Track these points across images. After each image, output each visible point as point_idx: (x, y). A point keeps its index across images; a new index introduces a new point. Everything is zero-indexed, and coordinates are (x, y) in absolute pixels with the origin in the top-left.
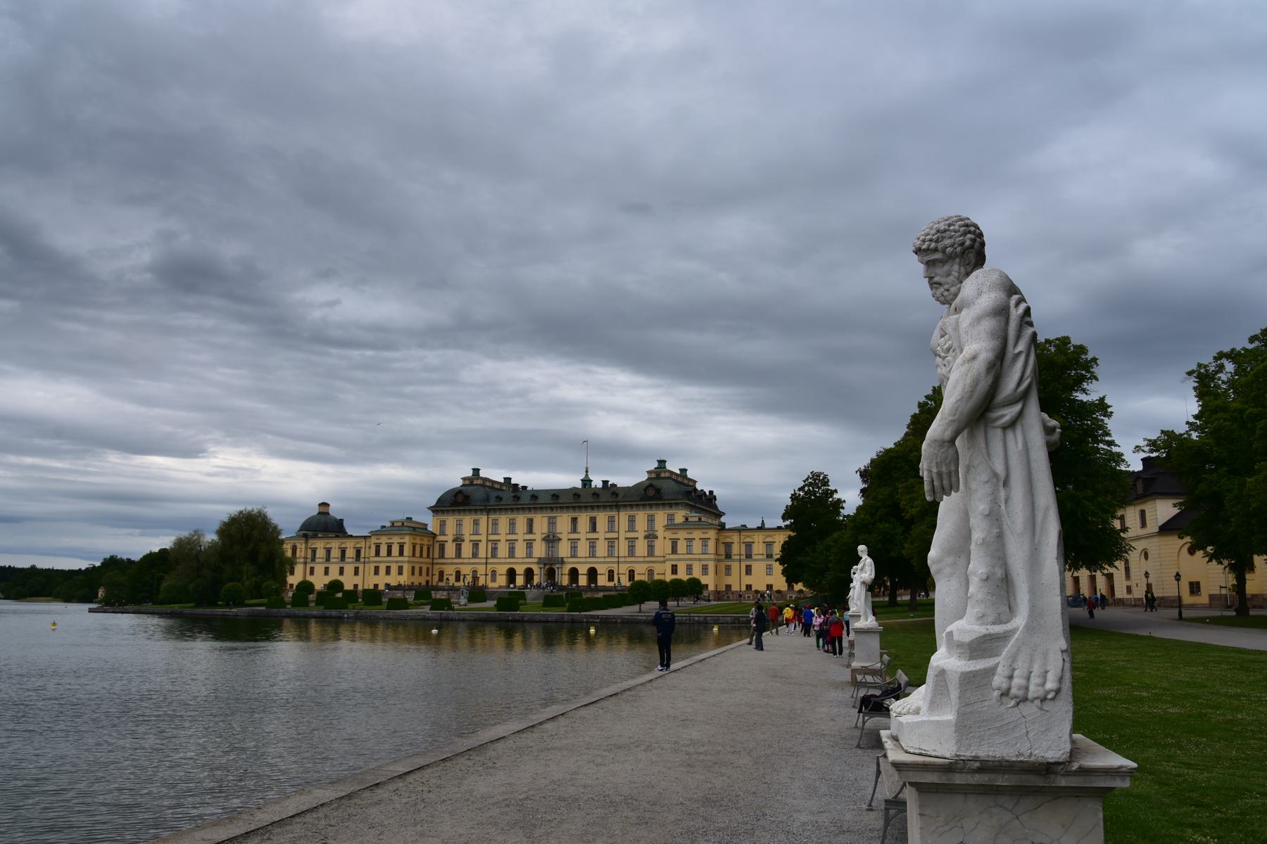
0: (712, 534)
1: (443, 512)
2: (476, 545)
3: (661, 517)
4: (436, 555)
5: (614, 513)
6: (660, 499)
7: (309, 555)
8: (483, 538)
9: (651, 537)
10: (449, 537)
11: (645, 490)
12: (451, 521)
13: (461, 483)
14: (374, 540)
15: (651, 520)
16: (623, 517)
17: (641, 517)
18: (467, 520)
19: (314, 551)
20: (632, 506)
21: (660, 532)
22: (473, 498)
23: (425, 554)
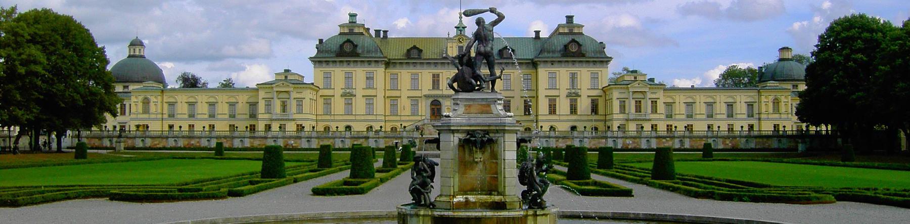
2: (370, 100)
3: (584, 74)
4: (320, 112)
6: (583, 56)
7: (166, 111)
8: (381, 95)
9: (573, 97)
10: (338, 92)
11: (566, 47)
12: (338, 73)
14: (262, 94)
15: (573, 77)
18: (359, 73)
19: (172, 105)
20: (552, 63)
22: (347, 48)
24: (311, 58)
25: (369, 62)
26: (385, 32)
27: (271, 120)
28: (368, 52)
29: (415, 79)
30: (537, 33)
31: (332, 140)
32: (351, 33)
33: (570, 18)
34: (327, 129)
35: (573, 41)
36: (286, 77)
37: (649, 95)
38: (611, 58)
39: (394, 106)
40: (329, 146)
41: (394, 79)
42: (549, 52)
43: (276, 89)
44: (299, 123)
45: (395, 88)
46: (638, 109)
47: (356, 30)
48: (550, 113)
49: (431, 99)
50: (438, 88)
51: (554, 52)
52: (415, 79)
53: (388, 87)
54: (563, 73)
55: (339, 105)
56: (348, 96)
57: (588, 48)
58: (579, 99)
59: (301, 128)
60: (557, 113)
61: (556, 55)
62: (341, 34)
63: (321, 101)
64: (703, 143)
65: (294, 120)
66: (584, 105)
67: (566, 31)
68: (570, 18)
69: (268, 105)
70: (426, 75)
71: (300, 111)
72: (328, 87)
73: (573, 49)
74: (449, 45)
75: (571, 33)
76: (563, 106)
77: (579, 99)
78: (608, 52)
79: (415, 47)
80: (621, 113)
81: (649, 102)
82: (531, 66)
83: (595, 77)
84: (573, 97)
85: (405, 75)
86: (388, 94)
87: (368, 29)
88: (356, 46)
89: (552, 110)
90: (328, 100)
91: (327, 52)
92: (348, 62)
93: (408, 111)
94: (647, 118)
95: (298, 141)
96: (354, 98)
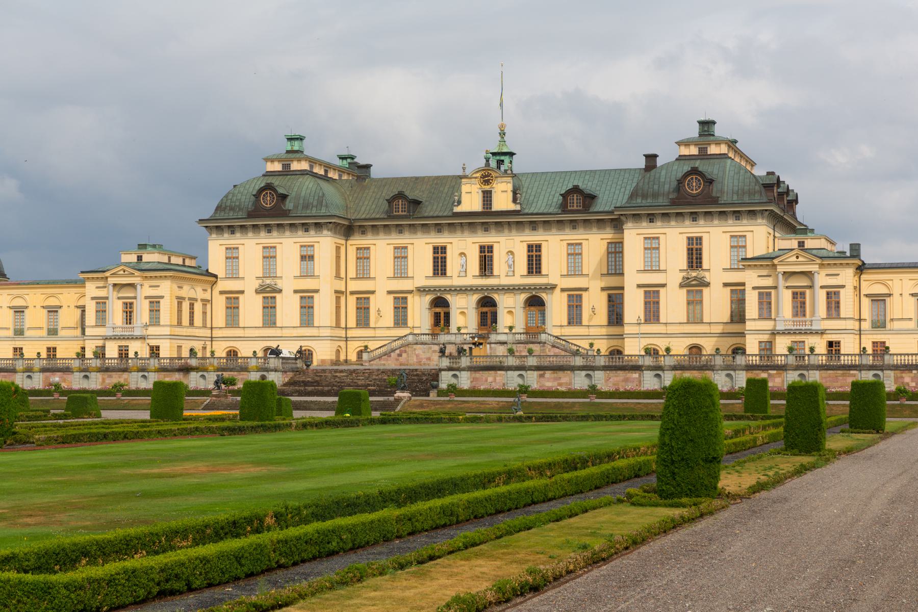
0: (847, 276)
1: (232, 230)
3: (717, 238)
6: (715, 201)
9: (695, 286)
16: (634, 237)
18: (288, 246)
20: (651, 218)
23: (198, 321)
25: (306, 227)
27: (106, 338)
28: (306, 206)
29: (401, 255)
30: (651, 158)
31: (125, 375)
34: (232, 354)
35: (694, 171)
36: (140, 258)
37: (822, 279)
39: (363, 311)
40: (175, 386)
41: (363, 256)
42: (645, 196)
43: (112, 281)
44: (154, 343)
45: (363, 274)
46: (800, 307)
47: (295, 166)
48: (647, 321)
49: (429, 298)
50: (444, 273)
51: (655, 195)
52: (401, 255)
53: (352, 273)
54: (674, 238)
55: (251, 308)
56: (269, 293)
57: (728, 183)
58: (706, 291)
59: (155, 351)
60: (663, 319)
61: (661, 201)
63: (220, 303)
64: (850, 380)
65: (143, 338)
66: (716, 303)
67: (694, 150)
69: (101, 312)
70: (421, 247)
71: (155, 320)
72: (233, 275)
73: (694, 188)
74: (465, 188)
76: (674, 304)
77: (706, 291)
79: (400, 195)
80: (761, 318)
81: (821, 295)
84: (695, 286)
85: (382, 248)
86: (354, 286)
88: (284, 197)
89: (652, 312)
91: (232, 209)
92: (269, 228)
93: (388, 318)
94: (815, 327)
95: (68, 377)
96: (278, 296)
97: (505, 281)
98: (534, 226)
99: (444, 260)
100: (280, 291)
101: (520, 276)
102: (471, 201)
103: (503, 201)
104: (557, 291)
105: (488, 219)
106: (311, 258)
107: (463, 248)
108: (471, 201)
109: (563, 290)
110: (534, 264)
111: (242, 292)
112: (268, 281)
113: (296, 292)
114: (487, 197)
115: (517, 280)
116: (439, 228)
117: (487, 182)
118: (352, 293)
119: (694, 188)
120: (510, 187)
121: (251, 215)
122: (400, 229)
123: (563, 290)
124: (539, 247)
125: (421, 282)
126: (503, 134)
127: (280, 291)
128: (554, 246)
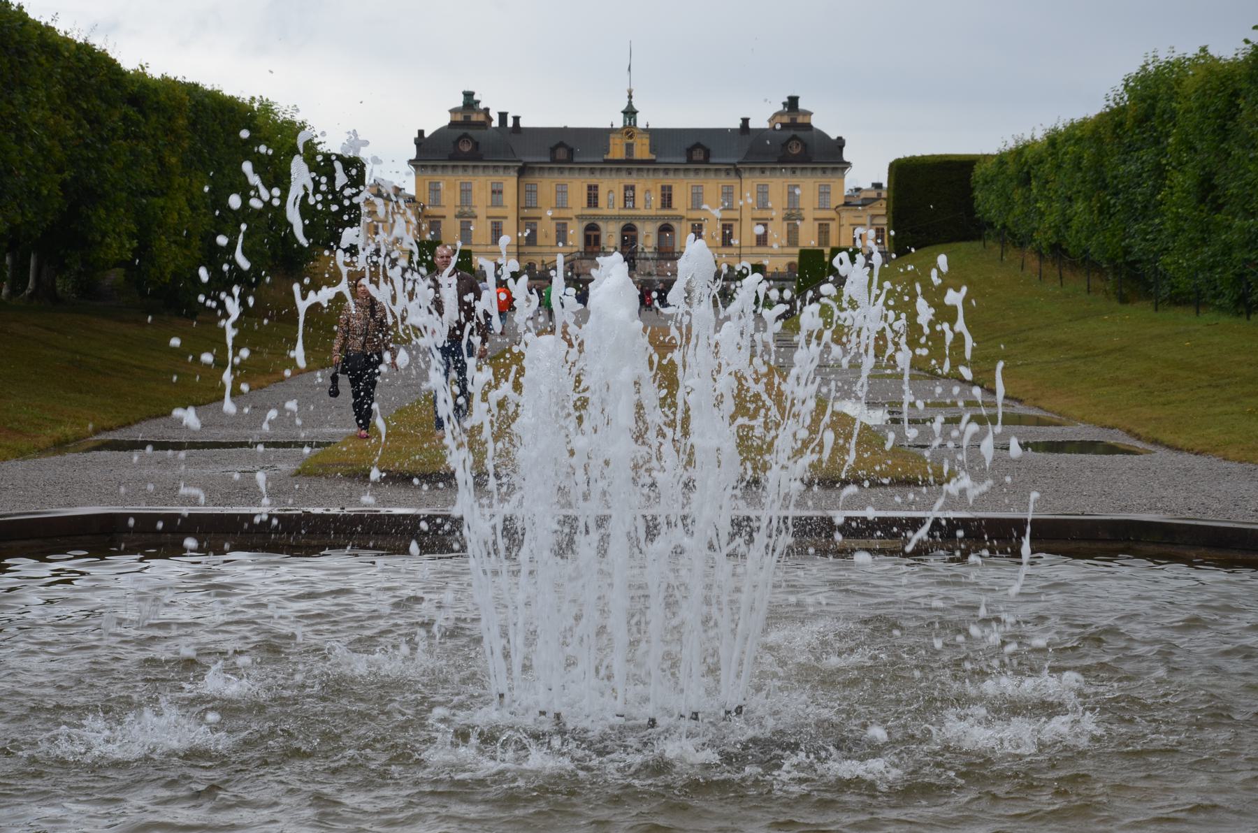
3: (807, 187)
5: (733, 181)
6: (809, 162)
12: (450, 183)
13: (445, 120)
17: (778, 185)
18: (481, 183)
21: (809, 214)
24: (410, 162)
26: (516, 119)
32: (467, 123)
33: (792, 102)
38: (849, 164)
41: (532, 192)
47: (474, 118)
49: (585, 223)
50: (596, 205)
52: (562, 191)
62: (453, 124)
67: (786, 120)
68: (792, 102)
70: (577, 186)
72: (436, 203)
75: (793, 125)
78: (847, 155)
82: (733, 174)
83: (824, 192)
85: (546, 185)
87: (487, 110)
90: (435, 224)
96: (474, 221)
97: (642, 212)
98: (666, 171)
99: (596, 197)
100: (476, 217)
101: (655, 207)
102: (617, 151)
103: (642, 150)
104: (684, 222)
105: (629, 164)
106: (500, 192)
107: (611, 187)
108: (617, 151)
109: (689, 220)
110: (667, 201)
111: (444, 217)
112: (466, 209)
113: (488, 217)
114: (629, 147)
115: (652, 212)
116: (592, 171)
117: (631, 137)
118: (523, 218)
119: (795, 150)
120: (647, 141)
121: (451, 159)
122: (561, 170)
123: (689, 220)
124: (670, 188)
125: (579, 213)
126: (630, 97)
127: (476, 217)
128: (682, 188)
